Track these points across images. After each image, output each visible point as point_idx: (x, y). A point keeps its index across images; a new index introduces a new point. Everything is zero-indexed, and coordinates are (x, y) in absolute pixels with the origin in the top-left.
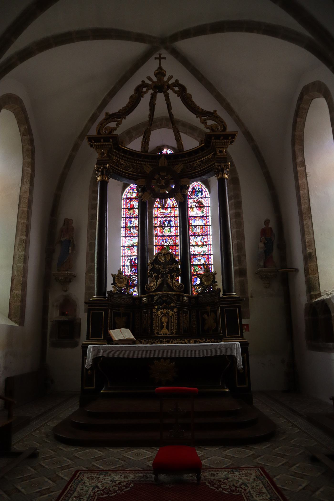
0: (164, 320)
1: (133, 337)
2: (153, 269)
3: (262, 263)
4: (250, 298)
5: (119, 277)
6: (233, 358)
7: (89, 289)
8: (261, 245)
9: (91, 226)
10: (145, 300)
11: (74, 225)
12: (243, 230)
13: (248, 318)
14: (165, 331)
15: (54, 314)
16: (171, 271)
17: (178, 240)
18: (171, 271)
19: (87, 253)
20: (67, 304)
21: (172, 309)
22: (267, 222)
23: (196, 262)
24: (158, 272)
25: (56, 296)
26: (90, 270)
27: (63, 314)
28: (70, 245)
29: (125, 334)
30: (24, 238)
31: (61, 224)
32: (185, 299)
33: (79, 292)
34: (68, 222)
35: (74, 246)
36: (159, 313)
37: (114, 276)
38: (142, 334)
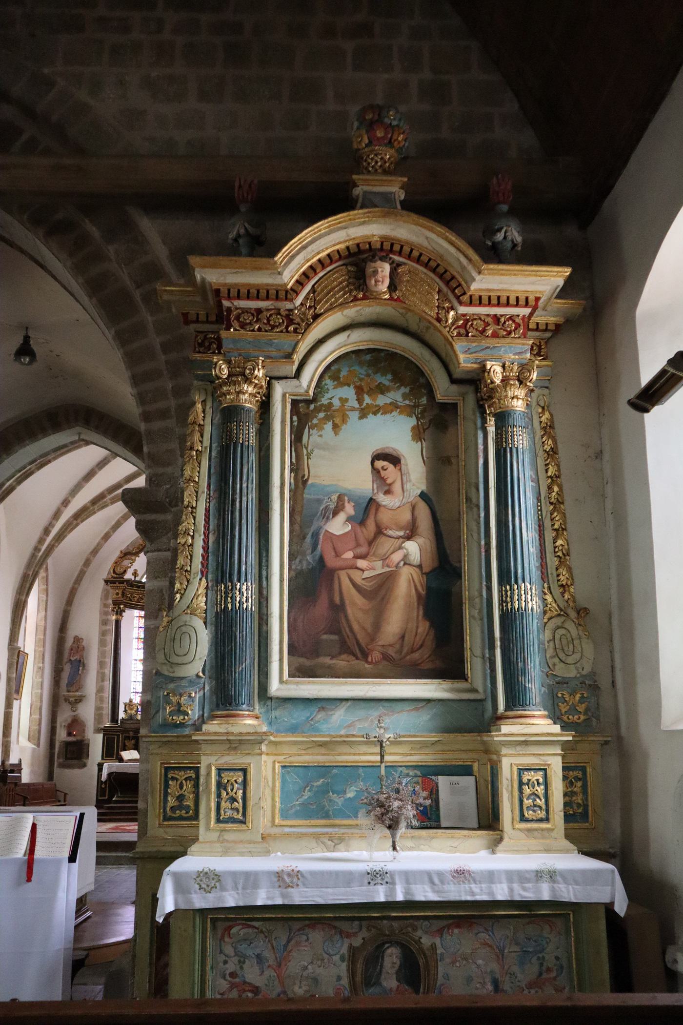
5: (129, 705)
7: (98, 709)
9: (102, 643)
11: (84, 643)
15: (62, 735)
19: (98, 672)
20: (75, 724)
25: (65, 716)
26: (100, 690)
27: (69, 734)
28: (79, 665)
30: (41, 665)
31: (69, 642)
33: (87, 712)
34: (77, 640)
35: (84, 666)
37: (126, 705)
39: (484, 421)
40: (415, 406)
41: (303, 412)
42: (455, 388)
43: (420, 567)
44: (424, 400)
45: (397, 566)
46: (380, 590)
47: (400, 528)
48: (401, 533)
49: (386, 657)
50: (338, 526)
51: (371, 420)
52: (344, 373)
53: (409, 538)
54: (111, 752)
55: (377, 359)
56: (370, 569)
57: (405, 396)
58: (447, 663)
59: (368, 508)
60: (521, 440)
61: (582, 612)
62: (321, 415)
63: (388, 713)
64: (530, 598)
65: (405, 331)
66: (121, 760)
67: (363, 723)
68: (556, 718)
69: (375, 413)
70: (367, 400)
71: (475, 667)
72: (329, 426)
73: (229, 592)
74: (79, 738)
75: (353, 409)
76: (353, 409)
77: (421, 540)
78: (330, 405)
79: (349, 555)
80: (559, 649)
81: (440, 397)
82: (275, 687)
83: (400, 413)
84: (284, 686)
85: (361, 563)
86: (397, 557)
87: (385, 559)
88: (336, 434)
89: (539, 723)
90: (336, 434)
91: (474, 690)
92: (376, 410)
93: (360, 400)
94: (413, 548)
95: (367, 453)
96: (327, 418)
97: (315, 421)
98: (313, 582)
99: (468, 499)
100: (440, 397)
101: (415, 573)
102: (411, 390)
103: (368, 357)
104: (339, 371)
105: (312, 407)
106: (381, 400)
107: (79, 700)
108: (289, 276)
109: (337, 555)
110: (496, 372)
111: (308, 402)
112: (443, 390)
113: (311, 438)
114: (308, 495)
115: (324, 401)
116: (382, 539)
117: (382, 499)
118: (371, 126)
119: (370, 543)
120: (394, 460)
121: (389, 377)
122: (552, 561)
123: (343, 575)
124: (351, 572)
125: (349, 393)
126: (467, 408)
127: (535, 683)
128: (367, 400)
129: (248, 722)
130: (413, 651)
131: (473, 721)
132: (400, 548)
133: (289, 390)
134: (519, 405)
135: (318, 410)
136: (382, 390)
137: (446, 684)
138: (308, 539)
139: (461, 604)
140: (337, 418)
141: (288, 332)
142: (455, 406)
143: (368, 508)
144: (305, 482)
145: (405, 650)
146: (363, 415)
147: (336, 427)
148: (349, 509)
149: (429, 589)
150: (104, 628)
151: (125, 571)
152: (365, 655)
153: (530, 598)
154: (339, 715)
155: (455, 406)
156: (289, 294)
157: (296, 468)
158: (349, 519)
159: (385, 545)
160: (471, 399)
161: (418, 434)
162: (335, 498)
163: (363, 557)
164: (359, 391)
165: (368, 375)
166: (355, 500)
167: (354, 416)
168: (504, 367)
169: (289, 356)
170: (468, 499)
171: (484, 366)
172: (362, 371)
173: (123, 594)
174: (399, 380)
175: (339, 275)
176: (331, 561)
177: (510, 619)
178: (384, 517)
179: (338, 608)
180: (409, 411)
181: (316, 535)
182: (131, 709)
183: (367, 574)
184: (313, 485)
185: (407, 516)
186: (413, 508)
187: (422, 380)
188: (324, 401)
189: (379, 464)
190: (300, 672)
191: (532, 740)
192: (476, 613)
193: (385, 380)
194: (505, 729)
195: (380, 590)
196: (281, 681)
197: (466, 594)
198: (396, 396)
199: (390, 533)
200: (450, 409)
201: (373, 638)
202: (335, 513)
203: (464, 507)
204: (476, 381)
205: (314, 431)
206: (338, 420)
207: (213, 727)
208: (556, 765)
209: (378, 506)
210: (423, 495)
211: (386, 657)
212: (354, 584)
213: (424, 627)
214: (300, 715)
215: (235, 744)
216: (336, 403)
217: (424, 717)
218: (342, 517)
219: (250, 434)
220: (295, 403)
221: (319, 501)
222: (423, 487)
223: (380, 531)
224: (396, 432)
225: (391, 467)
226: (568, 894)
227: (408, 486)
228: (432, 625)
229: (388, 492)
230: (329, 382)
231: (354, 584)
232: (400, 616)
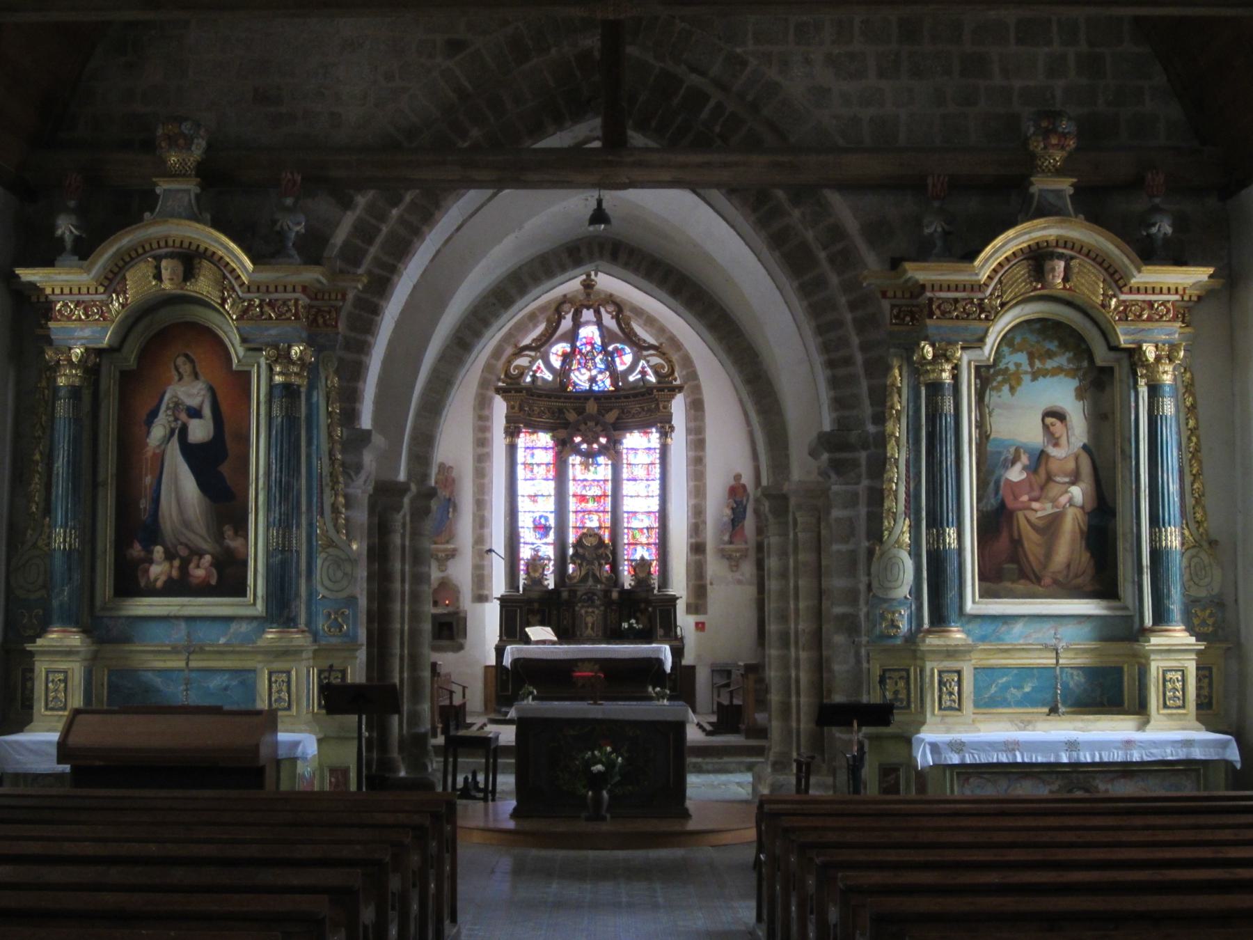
0: (589, 619)
1: (555, 639)
2: (576, 554)
3: (726, 538)
4: (709, 587)
6: (660, 662)
8: (728, 512)
10: (565, 595)
11: (454, 474)
12: (705, 485)
13: (705, 613)
14: (589, 631)
16: (599, 557)
17: (609, 486)
18: (599, 557)
19: (474, 515)
21: (597, 608)
22: (738, 477)
23: (635, 524)
24: (583, 558)
29: (540, 633)
32: (615, 595)
34: (442, 467)
35: (455, 509)
36: (583, 611)
38: (564, 635)
39: (1136, 383)
40: (1078, 369)
41: (986, 376)
42: (1112, 355)
43: (1082, 508)
44: (1085, 364)
45: (1064, 507)
46: (1051, 526)
47: (1066, 475)
48: (1067, 480)
49: (1055, 582)
50: (1016, 474)
51: (1042, 382)
52: (1018, 340)
53: (1073, 483)
54: (512, 629)
55: (1045, 327)
56: (1042, 509)
57: (1069, 361)
58: (1103, 583)
59: (1039, 459)
60: (1168, 407)
61: (1213, 543)
62: (1000, 378)
63: (1055, 625)
64: (1173, 538)
65: (1068, 303)
66: (526, 640)
67: (1046, 633)
68: (1190, 629)
69: (1044, 376)
70: (1038, 364)
71: (1126, 590)
72: (1006, 388)
73: (941, 535)
74: (451, 609)
75: (1026, 373)
76: (1026, 373)
77: (1083, 485)
78: (1007, 369)
79: (1025, 498)
80: (1194, 574)
81: (1099, 362)
82: (969, 607)
83: (1066, 375)
84: (976, 606)
85: (1035, 505)
86: (1064, 500)
87: (1054, 501)
88: (1013, 394)
89: (1179, 636)
90: (1013, 394)
91: (1126, 608)
92: (1045, 373)
93: (1032, 364)
94: (1077, 492)
95: (1037, 412)
96: (1004, 381)
97: (995, 384)
98: (995, 521)
99: (1123, 451)
100: (1099, 362)
101: (1079, 513)
102: (1075, 354)
103: (1038, 326)
104: (1013, 338)
105: (992, 371)
106: (1050, 364)
107: (452, 554)
108: (983, 277)
109: (1016, 498)
110: (1150, 352)
111: (988, 367)
112: (1102, 356)
113: (992, 398)
114: (990, 448)
115: (1002, 366)
116: (1052, 484)
117: (1052, 451)
118: (1046, 133)
119: (1042, 488)
120: (1060, 416)
121: (1056, 343)
122: (1190, 501)
123: (1020, 515)
124: (1027, 512)
125: (1022, 358)
126: (1121, 372)
127: (1175, 606)
128: (1038, 364)
129: (957, 635)
130: (1076, 576)
131: (1125, 632)
132: (1066, 492)
133: (973, 358)
134: (1167, 379)
135: (997, 373)
136: (1050, 355)
137: (1103, 603)
138: (992, 485)
139: (1115, 539)
140: (1013, 380)
141: (980, 319)
142: (1111, 369)
143: (1039, 459)
144: (988, 437)
145: (1071, 575)
146: (1035, 377)
147: (1012, 389)
148: (1025, 459)
149: (1090, 527)
150: (480, 450)
151: (522, 374)
152: (1038, 580)
153: (1173, 538)
154: (1018, 628)
155: (1111, 369)
156: (981, 287)
157: (981, 425)
158: (1025, 468)
159: (1054, 490)
160: (1126, 364)
161: (1080, 394)
162: (1012, 450)
163: (1036, 500)
164: (1031, 357)
165: (1038, 342)
166: (1030, 452)
167: (1027, 378)
168: (1157, 347)
169: (982, 340)
170: (1123, 451)
171: (1140, 347)
172: (1032, 338)
173: (521, 409)
174: (1064, 345)
175: (1022, 271)
176: (1010, 504)
177: (1158, 555)
178: (1053, 466)
179: (1017, 543)
180: (1072, 374)
181: (997, 483)
182: (535, 571)
183: (1039, 514)
184: (995, 439)
185: (1071, 465)
186: (1077, 458)
187: (1084, 346)
188: (1002, 366)
189: (1049, 420)
190: (986, 594)
191: (1174, 649)
192: (1128, 546)
193: (1053, 346)
194: (1154, 640)
195: (1051, 526)
196: (974, 602)
197: (1120, 531)
198: (1062, 360)
199: (1058, 479)
200: (1107, 371)
201: (1045, 567)
202: (1013, 463)
203: (1119, 458)
204: (1134, 355)
205: (994, 393)
206: (1013, 382)
207: (933, 641)
208: (1191, 667)
209: (1048, 456)
210: (1085, 447)
211: (1055, 582)
212: (1028, 521)
213: (1086, 557)
214: (989, 628)
215: (952, 653)
216: (1012, 368)
217: (1086, 629)
218: (1018, 466)
219: (948, 406)
220: (977, 368)
221: (1000, 453)
222: (1085, 440)
223: (1049, 478)
224: (1061, 392)
225: (1058, 423)
226: (1198, 754)
227: (1073, 440)
228: (1093, 555)
229: (1056, 445)
230: (1005, 349)
231: (1028, 521)
232: (1067, 548)
